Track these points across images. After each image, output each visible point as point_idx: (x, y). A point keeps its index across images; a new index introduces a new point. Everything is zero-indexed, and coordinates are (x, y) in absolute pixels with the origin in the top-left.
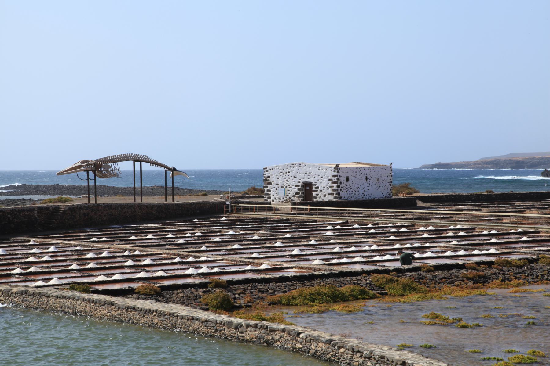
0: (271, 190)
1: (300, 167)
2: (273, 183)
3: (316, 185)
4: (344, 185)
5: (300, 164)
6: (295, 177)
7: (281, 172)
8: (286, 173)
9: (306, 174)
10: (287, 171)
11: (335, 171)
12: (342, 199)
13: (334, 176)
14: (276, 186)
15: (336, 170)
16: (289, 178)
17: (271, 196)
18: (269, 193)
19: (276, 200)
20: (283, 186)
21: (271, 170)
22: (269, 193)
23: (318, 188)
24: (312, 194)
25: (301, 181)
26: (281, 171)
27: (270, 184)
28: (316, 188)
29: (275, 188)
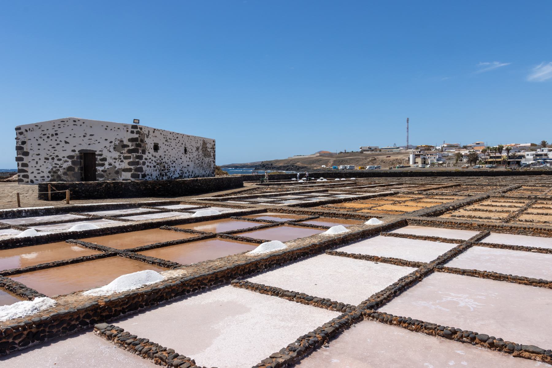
0: (29, 164)
1: (74, 125)
2: (31, 153)
3: (101, 155)
4: (150, 156)
5: (75, 121)
6: (66, 142)
7: (44, 135)
8: (52, 135)
9: (84, 136)
10: (54, 133)
11: (132, 132)
12: (147, 178)
13: (131, 140)
15: (135, 130)
16: (58, 144)
17: (29, 174)
18: (25, 168)
19: (37, 180)
20: (48, 157)
21: (26, 131)
22: (25, 168)
23: (105, 159)
24: (96, 170)
25: (77, 149)
26: (43, 133)
27: (27, 154)
28: (102, 160)
29: (35, 162)
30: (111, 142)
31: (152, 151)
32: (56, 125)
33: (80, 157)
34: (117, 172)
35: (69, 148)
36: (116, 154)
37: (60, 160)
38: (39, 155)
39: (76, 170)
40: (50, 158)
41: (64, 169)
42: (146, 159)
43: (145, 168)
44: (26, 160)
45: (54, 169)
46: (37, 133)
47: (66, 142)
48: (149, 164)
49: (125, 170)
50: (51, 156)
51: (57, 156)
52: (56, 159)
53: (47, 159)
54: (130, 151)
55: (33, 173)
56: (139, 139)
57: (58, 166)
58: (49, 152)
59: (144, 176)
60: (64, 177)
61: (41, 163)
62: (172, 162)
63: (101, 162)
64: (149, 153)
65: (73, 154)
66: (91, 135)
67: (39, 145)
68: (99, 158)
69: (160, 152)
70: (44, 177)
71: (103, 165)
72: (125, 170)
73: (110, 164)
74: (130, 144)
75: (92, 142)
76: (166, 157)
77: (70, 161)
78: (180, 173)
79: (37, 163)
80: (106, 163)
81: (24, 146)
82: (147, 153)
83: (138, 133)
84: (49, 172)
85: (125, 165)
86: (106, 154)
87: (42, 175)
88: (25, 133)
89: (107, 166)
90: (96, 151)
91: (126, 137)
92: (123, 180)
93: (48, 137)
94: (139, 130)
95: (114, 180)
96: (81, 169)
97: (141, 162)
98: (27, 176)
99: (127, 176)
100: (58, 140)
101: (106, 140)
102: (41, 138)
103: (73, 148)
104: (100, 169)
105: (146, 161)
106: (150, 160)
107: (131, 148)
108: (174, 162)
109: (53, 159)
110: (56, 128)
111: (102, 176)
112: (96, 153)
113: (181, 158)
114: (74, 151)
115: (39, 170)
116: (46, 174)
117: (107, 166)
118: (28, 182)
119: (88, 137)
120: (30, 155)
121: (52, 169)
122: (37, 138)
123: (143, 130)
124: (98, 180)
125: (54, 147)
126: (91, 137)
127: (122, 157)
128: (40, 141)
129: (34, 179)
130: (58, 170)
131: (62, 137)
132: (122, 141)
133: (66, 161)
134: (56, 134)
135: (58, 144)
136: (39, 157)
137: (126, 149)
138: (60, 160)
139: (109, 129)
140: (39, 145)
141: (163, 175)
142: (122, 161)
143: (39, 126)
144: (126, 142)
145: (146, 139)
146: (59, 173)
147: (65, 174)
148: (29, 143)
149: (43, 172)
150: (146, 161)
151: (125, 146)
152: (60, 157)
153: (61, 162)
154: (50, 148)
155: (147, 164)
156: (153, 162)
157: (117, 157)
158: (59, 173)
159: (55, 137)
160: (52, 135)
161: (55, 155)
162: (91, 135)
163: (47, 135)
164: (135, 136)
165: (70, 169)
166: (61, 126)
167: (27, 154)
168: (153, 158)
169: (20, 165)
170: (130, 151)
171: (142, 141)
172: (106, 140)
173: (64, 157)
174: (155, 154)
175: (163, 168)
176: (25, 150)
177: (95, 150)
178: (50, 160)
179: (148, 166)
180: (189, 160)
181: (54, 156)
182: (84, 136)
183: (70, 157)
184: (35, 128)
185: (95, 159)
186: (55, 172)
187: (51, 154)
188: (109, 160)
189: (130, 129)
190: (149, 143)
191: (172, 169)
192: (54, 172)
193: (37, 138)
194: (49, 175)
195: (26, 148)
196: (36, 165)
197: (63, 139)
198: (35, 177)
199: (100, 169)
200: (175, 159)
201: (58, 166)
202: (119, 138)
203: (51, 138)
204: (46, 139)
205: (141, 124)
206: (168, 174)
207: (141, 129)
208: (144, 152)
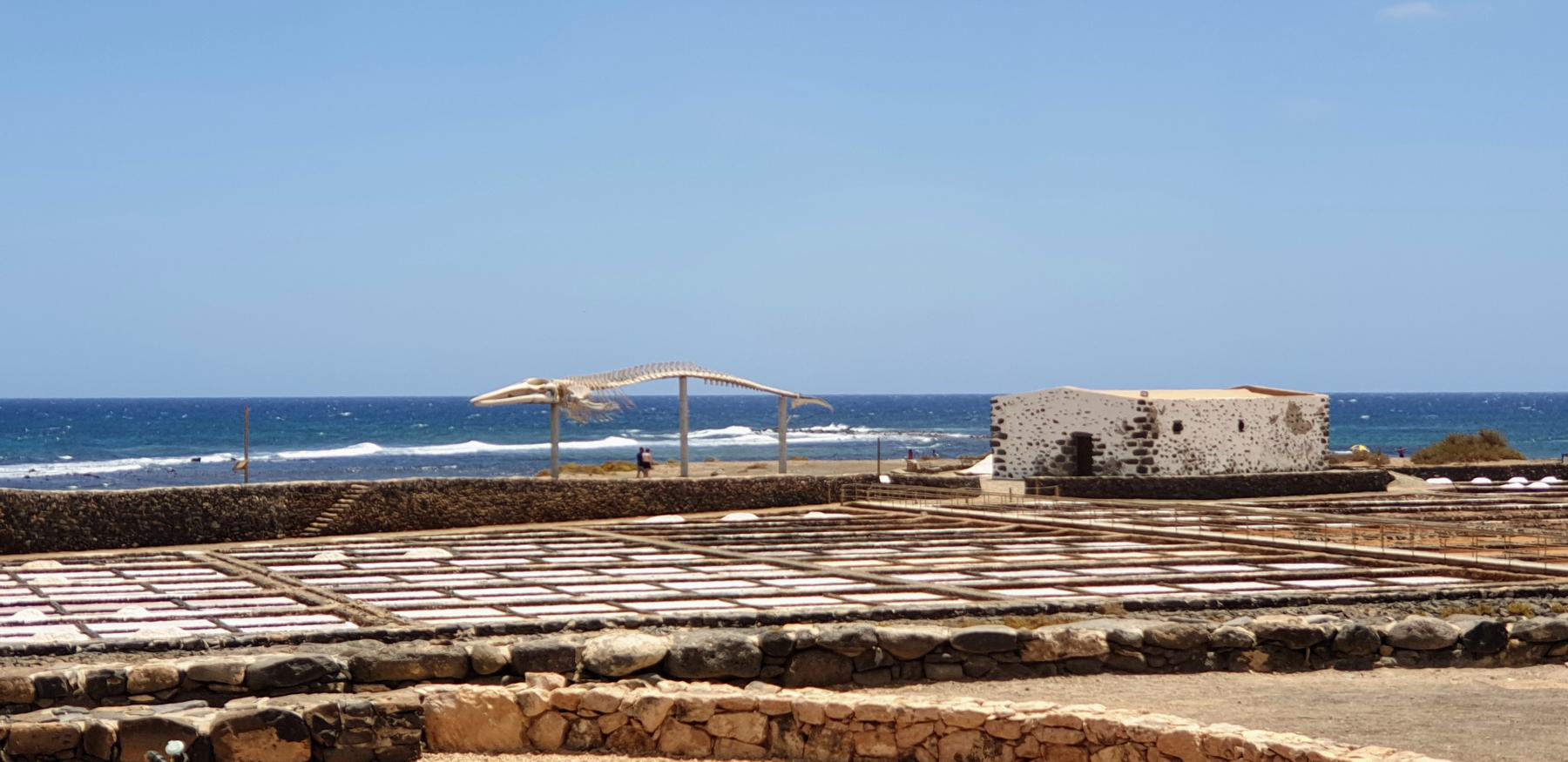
0: (1007, 450)
3: (1098, 440)
4: (1166, 441)
5: (1066, 393)
6: (1055, 422)
8: (1038, 411)
11: (1139, 409)
12: (1161, 473)
13: (1138, 420)
14: (1017, 442)
15: (1142, 407)
16: (1044, 424)
17: (1007, 465)
19: (1017, 473)
21: (1005, 405)
23: (1103, 446)
24: (1092, 461)
25: (1070, 431)
27: (1004, 437)
30: (1112, 423)
31: (1170, 434)
32: (1043, 397)
33: (1071, 443)
34: (1119, 465)
35: (1059, 429)
36: (1118, 439)
37: (1046, 446)
38: (1019, 438)
39: (1068, 460)
40: (1034, 443)
41: (1052, 458)
42: (1159, 446)
43: (1156, 458)
44: (1004, 444)
45: (1039, 459)
46: (1020, 408)
47: (1055, 422)
48: (1164, 453)
49: (1130, 462)
50: (1034, 440)
51: (1043, 440)
52: (1042, 444)
53: (1030, 444)
54: (1136, 436)
55: (1011, 463)
56: (1148, 419)
57: (1044, 455)
58: (1033, 435)
59: (1156, 470)
60: (1051, 470)
61: (1023, 449)
62: (1210, 447)
63: (1098, 450)
64: (1164, 436)
65: (1063, 438)
66: (1087, 412)
67: (1021, 424)
68: (1096, 444)
69: (1185, 434)
70: (1025, 469)
71: (1101, 454)
72: (1130, 462)
73: (1111, 453)
74: (1135, 425)
75: (1088, 421)
76: (1198, 440)
77: (1059, 447)
78: (1227, 464)
79: (1017, 449)
80: (1106, 451)
81: (1001, 426)
82: (1161, 437)
83: (1146, 410)
84: (1033, 463)
85: (1129, 455)
86: (1105, 439)
87: (1024, 466)
88: (1003, 407)
89: (1106, 456)
90: (1092, 435)
91: (1131, 415)
92: (1128, 475)
93: (1032, 414)
94: (1147, 406)
95: (1115, 474)
96: (1073, 459)
97: (1150, 450)
98: (1004, 468)
99: (1132, 469)
100: (1045, 418)
101: (1106, 419)
102: (1023, 414)
103: (1064, 430)
104: (1097, 459)
105: (1159, 449)
106: (1167, 448)
107: (1138, 430)
108: (1215, 447)
109: (1038, 444)
110: (1043, 402)
111: (1099, 469)
112: (1093, 437)
113: (1230, 440)
114: (1065, 434)
115: (1019, 459)
116: (1029, 466)
117: (1106, 456)
118: (1005, 476)
119: (1083, 415)
120: (1009, 438)
121: (1036, 458)
122: (1019, 414)
123: (1155, 405)
124: (1094, 475)
125: (1039, 428)
126: (1086, 415)
127: (1125, 443)
128: (1023, 419)
129: (1012, 472)
130: (1044, 460)
131: (1050, 414)
132: (1125, 422)
133: (1055, 448)
134: (1043, 410)
135: (1044, 424)
136: (1020, 441)
137: (1131, 432)
138: (1046, 446)
139: (1109, 404)
140: (1021, 424)
141: (1191, 469)
142: (1125, 449)
143: (1022, 398)
144: (1131, 423)
145: (1159, 417)
146: (1045, 464)
147: (1053, 465)
148: (1007, 421)
149: (1024, 462)
150: (1159, 449)
151: (1129, 428)
152: (1047, 442)
153: (1048, 449)
154: (1034, 429)
155: (1161, 452)
156: (1172, 449)
157: (1119, 443)
158: (1045, 464)
159: (1041, 413)
160: (1038, 411)
161: (1041, 438)
162: (1087, 412)
163: (1032, 411)
164: (1143, 414)
165: (1060, 459)
166: (1050, 399)
167: (1004, 437)
168: (1173, 445)
169: (996, 452)
170: (1136, 436)
171: (1152, 421)
172: (1106, 419)
173: (1052, 442)
174: (1175, 437)
175: (1190, 458)
176: (1003, 431)
177: (1090, 432)
178: (1035, 446)
179: (1162, 456)
180: (1250, 442)
181: (1039, 440)
182: (1078, 414)
183: (1061, 442)
184: (1017, 400)
185: (1092, 446)
186: (1040, 463)
187: (1036, 437)
188: (1109, 448)
189: (1137, 405)
190: (1165, 423)
191: (1209, 459)
192: (1039, 463)
193: (1019, 414)
194: (1033, 466)
195: (1004, 429)
196: (1015, 452)
197: (1052, 417)
198: (1015, 469)
199: (1097, 459)
200: (1216, 443)
201: (1044, 455)
202: (1122, 416)
203: (1036, 415)
204: (1030, 417)
205: (1150, 398)
206: (1200, 466)
207: (1151, 404)
208: (1155, 436)
